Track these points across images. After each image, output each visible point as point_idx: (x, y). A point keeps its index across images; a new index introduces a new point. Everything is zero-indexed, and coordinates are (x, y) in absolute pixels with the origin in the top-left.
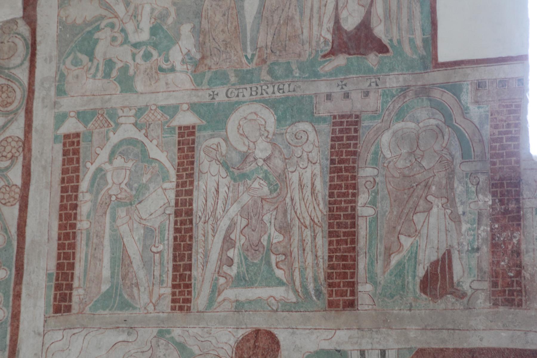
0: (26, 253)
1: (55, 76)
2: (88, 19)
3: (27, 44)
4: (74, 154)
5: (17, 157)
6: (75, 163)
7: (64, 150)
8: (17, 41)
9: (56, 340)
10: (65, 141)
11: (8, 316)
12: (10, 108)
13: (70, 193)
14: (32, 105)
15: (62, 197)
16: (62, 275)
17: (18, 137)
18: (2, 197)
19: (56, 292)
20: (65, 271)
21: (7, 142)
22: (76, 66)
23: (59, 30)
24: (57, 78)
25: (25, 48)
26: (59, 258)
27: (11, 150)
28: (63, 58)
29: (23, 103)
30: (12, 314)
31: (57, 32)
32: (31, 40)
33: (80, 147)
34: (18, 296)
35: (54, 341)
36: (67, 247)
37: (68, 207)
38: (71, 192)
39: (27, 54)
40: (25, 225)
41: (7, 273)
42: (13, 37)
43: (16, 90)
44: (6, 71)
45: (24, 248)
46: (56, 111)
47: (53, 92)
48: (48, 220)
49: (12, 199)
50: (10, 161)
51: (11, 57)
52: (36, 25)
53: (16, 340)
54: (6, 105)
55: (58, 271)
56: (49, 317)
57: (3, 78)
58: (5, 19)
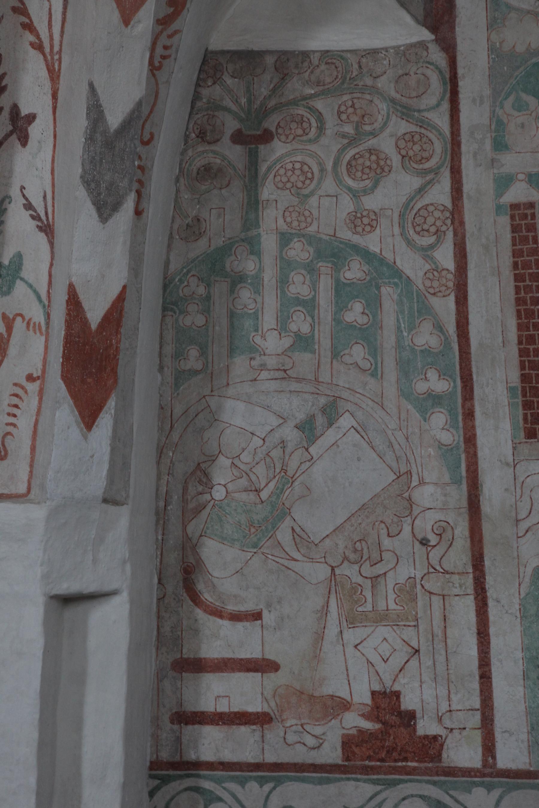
0: (473, 359)
1: (489, 124)
2: (533, 46)
3: (443, 78)
4: (528, 231)
5: (444, 232)
6: (531, 243)
7: (512, 225)
8: (429, 72)
9: (533, 473)
10: (513, 212)
11: (459, 441)
12: (427, 165)
13: (528, 283)
14: (460, 162)
15: (517, 289)
16: (530, 389)
17: (443, 205)
18: (430, 285)
19: (526, 412)
20: (534, 385)
21: (428, 211)
22: (519, 111)
23: (491, 60)
24: (493, 127)
25: (442, 83)
26: (522, 367)
27: (435, 222)
28: (500, 99)
29: (445, 158)
30: (465, 438)
31: (489, 63)
32: (449, 72)
33: (536, 221)
34: (469, 415)
35: (530, 474)
36: (532, 353)
37: (529, 302)
38: (530, 281)
39: (445, 91)
40: (468, 323)
41: (450, 384)
42: (422, 67)
43: (433, 142)
44: (416, 113)
45: (470, 353)
46: (496, 171)
47: (488, 145)
48: (499, 315)
49: (444, 288)
50: (435, 236)
51: (422, 94)
52: (456, 52)
53: (476, 471)
54: (420, 160)
55: (523, 385)
56: (520, 443)
57: (413, 124)
58: (408, 42)
